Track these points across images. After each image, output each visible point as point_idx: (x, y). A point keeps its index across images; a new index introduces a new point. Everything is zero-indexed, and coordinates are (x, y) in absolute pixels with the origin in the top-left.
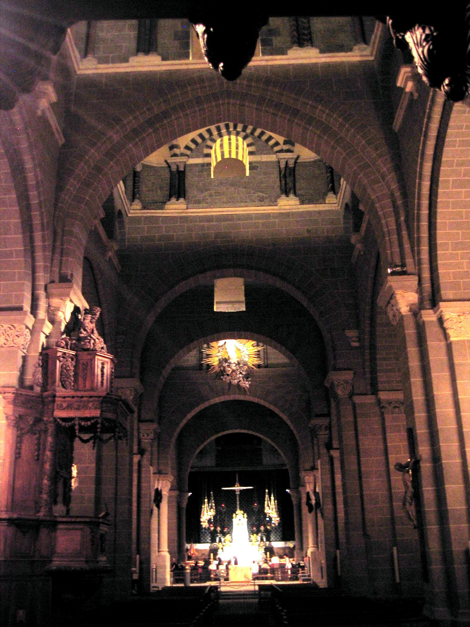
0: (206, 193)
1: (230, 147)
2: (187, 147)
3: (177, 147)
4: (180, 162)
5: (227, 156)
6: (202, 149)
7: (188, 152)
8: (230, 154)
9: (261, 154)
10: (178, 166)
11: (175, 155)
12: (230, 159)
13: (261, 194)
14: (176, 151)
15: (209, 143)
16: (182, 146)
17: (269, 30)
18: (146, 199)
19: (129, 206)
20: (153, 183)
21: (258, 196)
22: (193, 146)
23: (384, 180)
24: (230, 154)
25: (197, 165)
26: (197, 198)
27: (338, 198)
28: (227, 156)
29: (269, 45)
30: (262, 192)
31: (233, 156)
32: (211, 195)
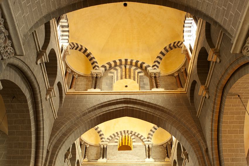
0: (115, 156)
1: (125, 141)
2: (108, 139)
3: (104, 138)
4: (105, 144)
5: (124, 144)
6: (114, 140)
7: (109, 141)
8: (125, 143)
9: (138, 142)
10: (104, 146)
11: (103, 141)
12: (125, 145)
13: (138, 157)
14: (103, 140)
15: (117, 137)
16: (106, 138)
17: (144, 84)
18: (90, 158)
19: (82, 159)
20: (93, 152)
21: (137, 158)
22: (110, 138)
23: (195, 137)
24: (125, 143)
25: (112, 146)
26: (111, 158)
27: (170, 159)
28: (124, 144)
29: (144, 88)
30: (138, 157)
31: (126, 144)
32: (117, 157)
